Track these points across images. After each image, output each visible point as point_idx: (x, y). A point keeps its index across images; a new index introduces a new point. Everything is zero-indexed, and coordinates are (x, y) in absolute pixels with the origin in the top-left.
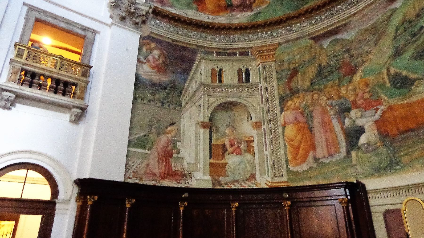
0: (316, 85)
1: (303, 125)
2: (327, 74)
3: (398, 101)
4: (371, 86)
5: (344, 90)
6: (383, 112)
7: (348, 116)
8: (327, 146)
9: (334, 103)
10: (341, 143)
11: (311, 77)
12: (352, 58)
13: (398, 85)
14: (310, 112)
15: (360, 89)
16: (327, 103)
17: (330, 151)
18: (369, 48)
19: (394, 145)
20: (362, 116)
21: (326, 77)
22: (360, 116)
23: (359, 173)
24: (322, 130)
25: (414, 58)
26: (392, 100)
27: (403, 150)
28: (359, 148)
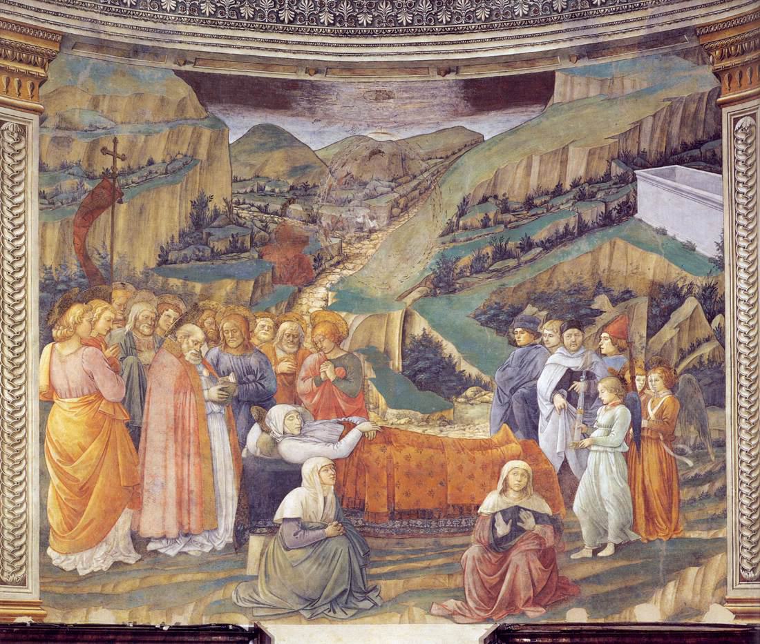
0: (176, 274)
1: (110, 411)
2: (220, 246)
3: (410, 422)
4: (346, 345)
5: (266, 328)
6: (364, 436)
7: (261, 420)
8: (179, 504)
9: (227, 361)
10: (223, 500)
11: (164, 239)
12: (311, 226)
13: (422, 376)
14: (140, 367)
15: (315, 344)
16: (203, 354)
17: (185, 521)
18: (372, 218)
19: (371, 541)
20: (302, 434)
21: (215, 255)
22: (297, 432)
23: (258, 603)
24: (171, 444)
25: (483, 318)
26: (395, 411)
27: (391, 562)
28: (273, 530)
